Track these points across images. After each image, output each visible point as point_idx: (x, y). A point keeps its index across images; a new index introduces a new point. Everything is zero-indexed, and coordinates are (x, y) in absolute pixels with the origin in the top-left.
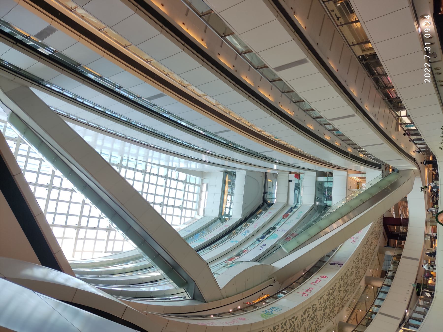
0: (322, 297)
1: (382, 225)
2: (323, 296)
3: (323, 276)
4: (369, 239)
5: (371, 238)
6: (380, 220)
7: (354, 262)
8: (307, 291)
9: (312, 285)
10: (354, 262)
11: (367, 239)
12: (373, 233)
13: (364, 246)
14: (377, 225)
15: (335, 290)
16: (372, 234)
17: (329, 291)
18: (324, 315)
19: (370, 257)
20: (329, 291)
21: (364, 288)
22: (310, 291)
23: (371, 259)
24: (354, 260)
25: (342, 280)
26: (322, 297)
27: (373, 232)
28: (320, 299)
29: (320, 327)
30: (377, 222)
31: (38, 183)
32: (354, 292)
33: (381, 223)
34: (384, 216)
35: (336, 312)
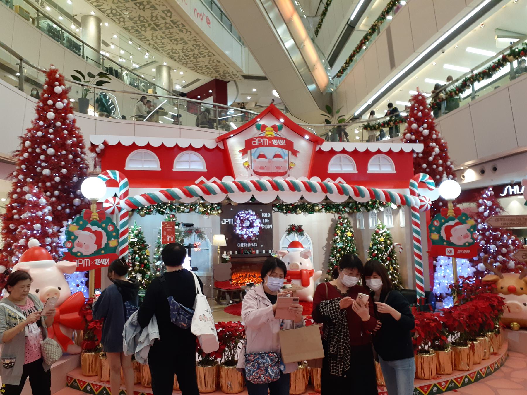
1: (212, 75)
4: (184, 31)
5: (186, 39)
6: (221, 69)
11: (183, 26)
12: (197, 45)
13: (169, 11)
14: (213, 61)
16: (195, 43)
19: (143, 33)
21: (72, 13)
23: (141, 39)
27: (198, 45)
30: (218, 62)
33: (216, 75)
34: (229, 82)
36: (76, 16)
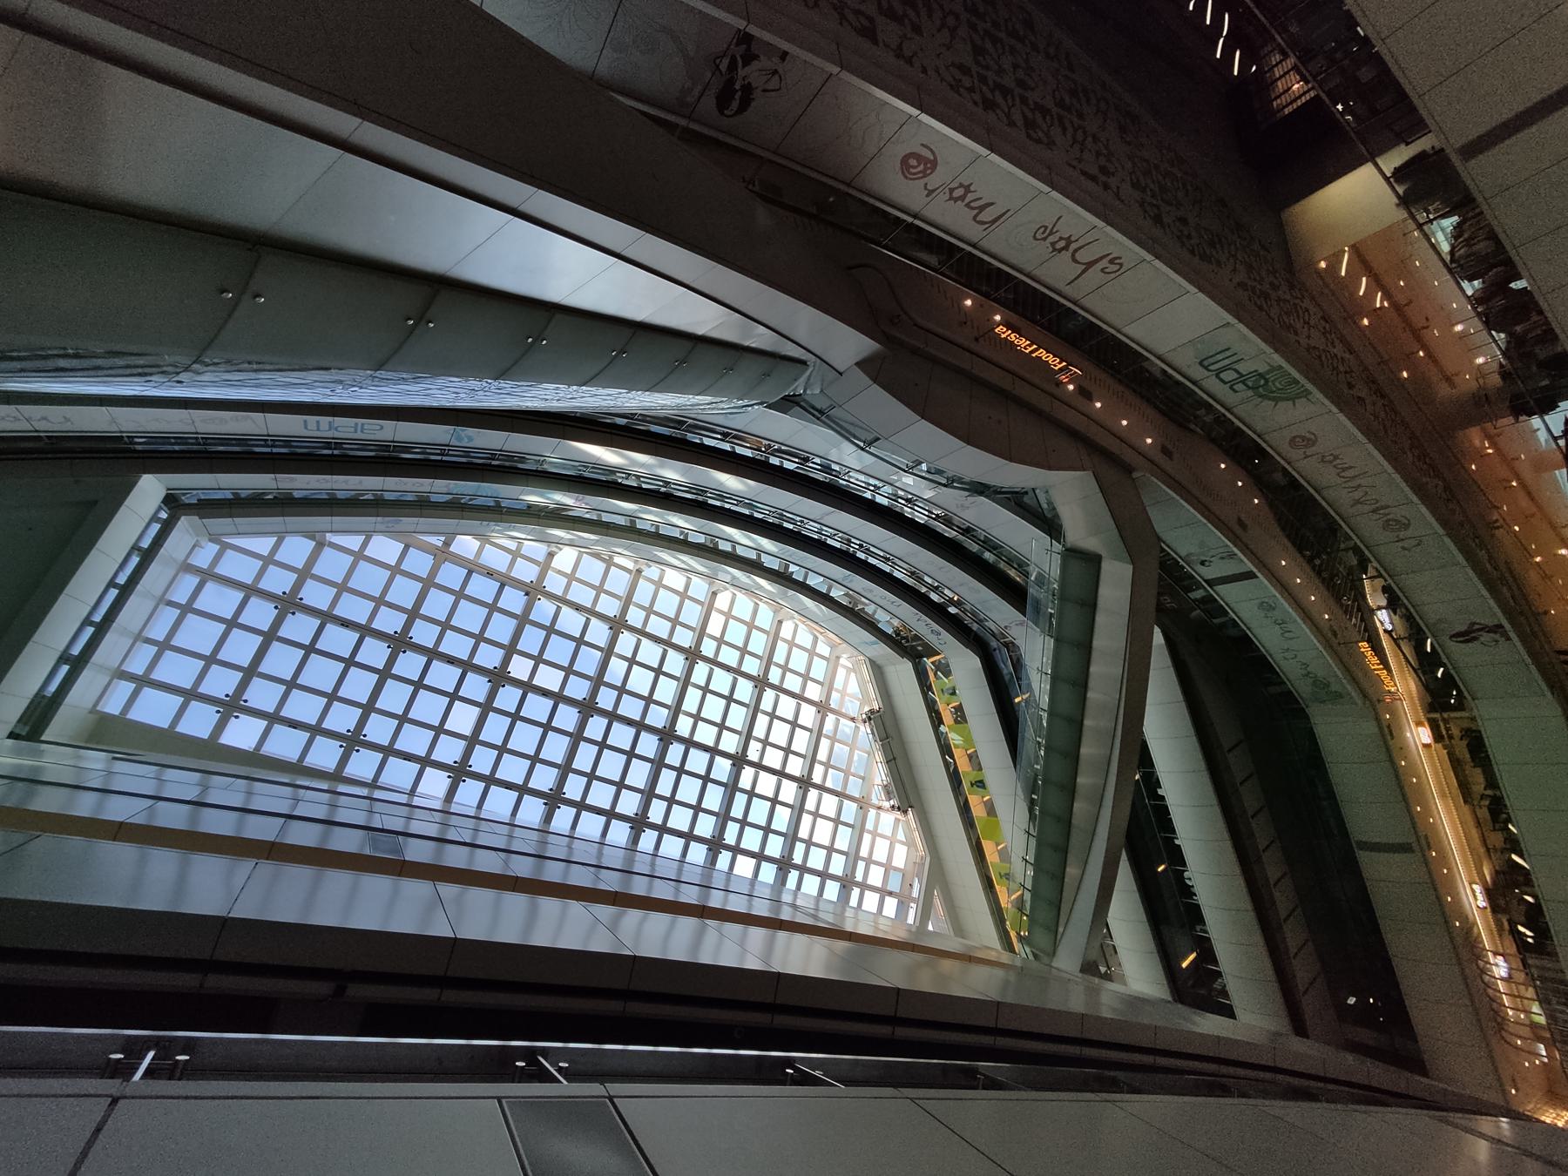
31: (551, 703)
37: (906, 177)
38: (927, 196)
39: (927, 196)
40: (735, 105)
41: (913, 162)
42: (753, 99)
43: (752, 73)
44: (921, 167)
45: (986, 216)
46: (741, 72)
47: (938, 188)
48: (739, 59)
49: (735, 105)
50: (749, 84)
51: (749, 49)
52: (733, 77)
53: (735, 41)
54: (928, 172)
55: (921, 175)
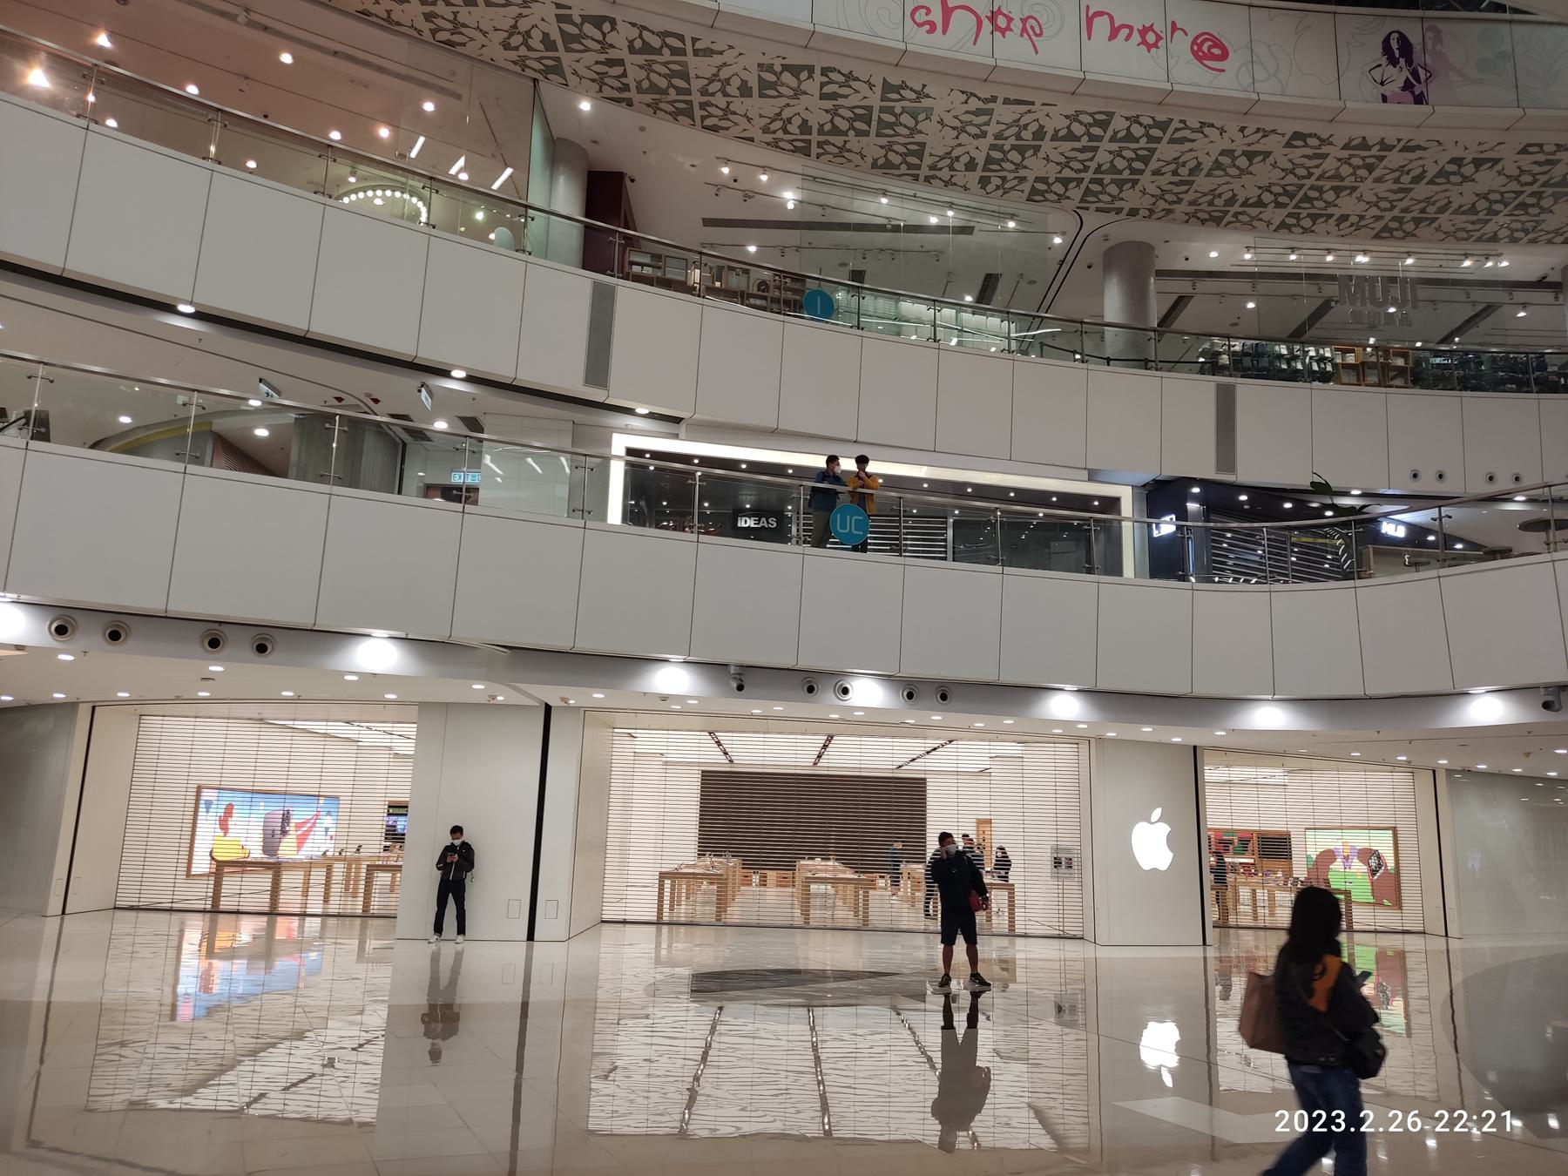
0: (1007, 101)
2: (1033, 103)
3: (1217, 43)
7: (1524, 151)
8: (984, 12)
9: (1073, 21)
10: (1524, 151)
15: (1172, 141)
17: (1111, 115)
18: (989, 160)
20: (1111, 115)
21: (1533, 277)
22: (996, 28)
24: (1541, 146)
25: (1288, 145)
26: (1007, 101)
28: (994, 99)
29: (924, 171)
32: (1377, 237)
35: (1127, 206)
36: (1545, 278)
37: (1210, 34)
38: (1174, 24)
39: (1174, 24)
40: (1394, 45)
41: (1216, 51)
42: (1384, 55)
43: (1398, 75)
44: (1205, 48)
45: (1101, 26)
46: (1406, 74)
47: (1172, 35)
48: (1415, 83)
49: (1394, 45)
50: (1395, 67)
51: (1413, 93)
52: (1410, 67)
53: (1426, 94)
54: (1195, 47)
55: (1199, 41)
